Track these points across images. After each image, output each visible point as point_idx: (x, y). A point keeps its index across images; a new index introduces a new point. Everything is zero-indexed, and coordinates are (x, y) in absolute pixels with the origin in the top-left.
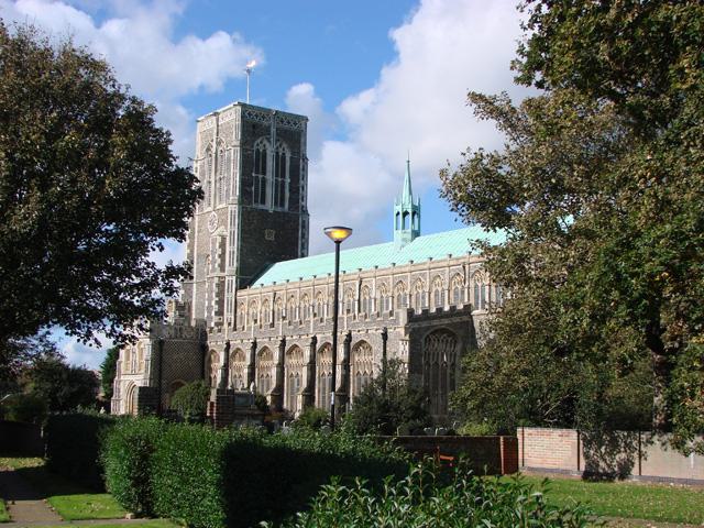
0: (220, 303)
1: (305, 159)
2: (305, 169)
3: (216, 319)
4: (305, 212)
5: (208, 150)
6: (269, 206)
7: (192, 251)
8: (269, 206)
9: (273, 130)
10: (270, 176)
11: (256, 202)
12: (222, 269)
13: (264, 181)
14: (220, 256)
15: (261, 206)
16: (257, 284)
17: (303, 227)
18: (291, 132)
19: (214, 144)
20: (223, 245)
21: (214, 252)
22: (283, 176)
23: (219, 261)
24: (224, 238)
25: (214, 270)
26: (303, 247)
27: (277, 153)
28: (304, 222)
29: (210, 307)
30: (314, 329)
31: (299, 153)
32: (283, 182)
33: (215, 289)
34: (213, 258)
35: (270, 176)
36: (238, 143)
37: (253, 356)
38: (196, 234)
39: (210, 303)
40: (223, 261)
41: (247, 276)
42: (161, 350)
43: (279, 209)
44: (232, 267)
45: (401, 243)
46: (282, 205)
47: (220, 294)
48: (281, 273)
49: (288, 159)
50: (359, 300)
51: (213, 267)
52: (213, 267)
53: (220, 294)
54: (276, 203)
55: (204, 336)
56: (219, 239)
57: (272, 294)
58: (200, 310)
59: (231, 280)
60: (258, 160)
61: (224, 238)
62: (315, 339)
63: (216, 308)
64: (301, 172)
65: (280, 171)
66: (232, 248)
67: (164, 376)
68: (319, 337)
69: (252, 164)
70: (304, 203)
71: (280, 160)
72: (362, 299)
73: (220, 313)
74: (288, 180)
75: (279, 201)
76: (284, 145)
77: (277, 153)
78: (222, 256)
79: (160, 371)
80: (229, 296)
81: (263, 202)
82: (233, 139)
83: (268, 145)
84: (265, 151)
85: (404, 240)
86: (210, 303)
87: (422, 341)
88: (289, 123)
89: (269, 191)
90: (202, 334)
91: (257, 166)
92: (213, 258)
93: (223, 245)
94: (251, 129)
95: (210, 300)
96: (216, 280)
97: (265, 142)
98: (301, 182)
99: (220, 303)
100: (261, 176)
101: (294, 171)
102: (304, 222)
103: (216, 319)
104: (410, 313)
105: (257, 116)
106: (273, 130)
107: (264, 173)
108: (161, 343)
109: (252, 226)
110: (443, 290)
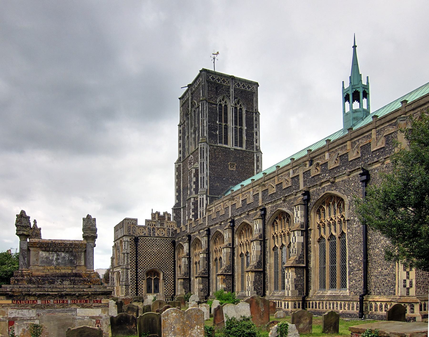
2: (257, 120)
4: (258, 150)
7: (179, 187)
8: (231, 145)
10: (231, 124)
13: (226, 128)
14: (194, 183)
15: (224, 146)
17: (258, 161)
22: (241, 125)
23: (194, 186)
24: (197, 170)
26: (258, 161)
27: (236, 108)
28: (258, 157)
30: (263, 200)
31: (252, 109)
32: (241, 129)
33: (192, 207)
35: (231, 124)
38: (182, 175)
40: (197, 186)
42: (137, 246)
43: (239, 148)
46: (241, 146)
52: (191, 192)
56: (194, 170)
59: (203, 198)
60: (220, 112)
62: (264, 210)
65: (238, 120)
70: (257, 144)
74: (245, 128)
75: (239, 141)
77: (236, 108)
78: (196, 183)
81: (226, 143)
84: (226, 106)
88: (243, 86)
91: (221, 116)
96: (192, 200)
98: (255, 129)
102: (258, 157)
107: (226, 121)
108: (136, 240)
109: (218, 160)
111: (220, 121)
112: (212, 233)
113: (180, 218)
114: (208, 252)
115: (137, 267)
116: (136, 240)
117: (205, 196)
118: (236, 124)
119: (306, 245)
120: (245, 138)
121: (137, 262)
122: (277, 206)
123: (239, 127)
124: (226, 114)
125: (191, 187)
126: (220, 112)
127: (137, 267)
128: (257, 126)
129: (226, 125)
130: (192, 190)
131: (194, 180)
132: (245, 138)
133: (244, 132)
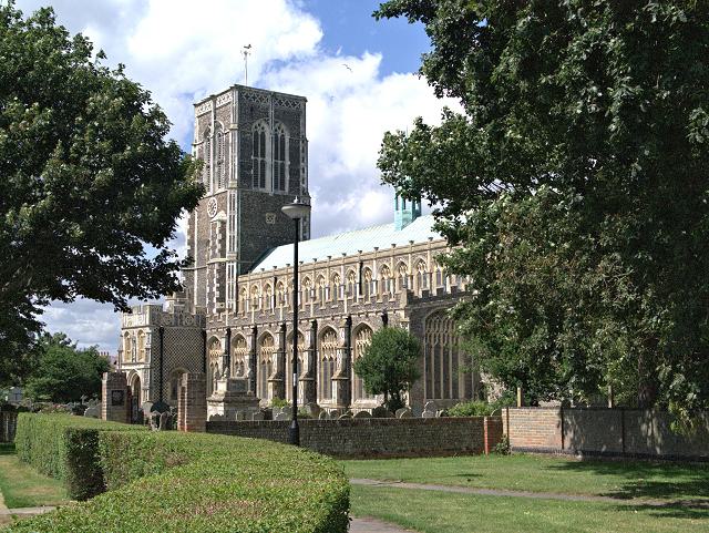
0: (222, 289)
1: (305, 141)
2: (305, 150)
3: (217, 305)
5: (207, 134)
6: (269, 189)
7: (193, 237)
9: (271, 112)
10: (269, 159)
11: (256, 185)
12: (223, 256)
14: (220, 241)
16: (257, 269)
18: (292, 111)
19: (212, 128)
20: (223, 230)
21: (214, 238)
23: (219, 246)
25: (214, 256)
29: (211, 293)
30: (314, 311)
31: (298, 135)
32: (283, 165)
34: (214, 243)
35: (269, 159)
36: (236, 126)
37: (254, 342)
39: (211, 289)
40: (224, 246)
41: (248, 261)
43: (279, 192)
44: (232, 253)
45: (401, 224)
46: (283, 188)
47: (222, 280)
48: (281, 257)
49: (287, 141)
50: (360, 284)
51: (214, 252)
52: (214, 252)
53: (222, 280)
54: (276, 187)
55: (203, 321)
56: (219, 225)
57: (273, 279)
58: (202, 292)
60: (256, 142)
61: (223, 223)
62: (315, 323)
63: (217, 294)
64: (301, 154)
66: (232, 233)
67: (165, 364)
68: (319, 321)
69: (250, 147)
71: (279, 143)
72: (363, 281)
73: (222, 299)
75: (279, 183)
76: (283, 127)
78: (223, 241)
79: (161, 359)
80: (230, 282)
81: (263, 186)
82: (231, 122)
83: (266, 126)
84: (263, 133)
85: (404, 220)
86: (211, 289)
87: (424, 322)
88: (287, 104)
89: (269, 175)
90: (202, 320)
91: (256, 148)
92: (214, 243)
93: (223, 230)
94: (248, 111)
95: (211, 285)
97: (264, 124)
98: (302, 164)
99: (222, 289)
100: (260, 159)
101: (296, 150)
103: (217, 305)
104: (410, 295)
105: (254, 98)
106: (271, 112)
107: (263, 155)
108: (161, 331)
110: (425, 273)
111: (256, 155)
112: (260, 333)
113: (193, 283)
114: (254, 354)
115: (161, 366)
116: (161, 331)
117: (235, 264)
118: (276, 158)
119: (347, 361)
120: (287, 177)
121: (161, 359)
122: (327, 322)
123: (280, 162)
124: (263, 144)
125: (214, 247)
126: (256, 142)
127: (161, 366)
128: (305, 159)
129: (262, 161)
130: (217, 251)
131: (220, 237)
132: (287, 177)
133: (287, 168)
